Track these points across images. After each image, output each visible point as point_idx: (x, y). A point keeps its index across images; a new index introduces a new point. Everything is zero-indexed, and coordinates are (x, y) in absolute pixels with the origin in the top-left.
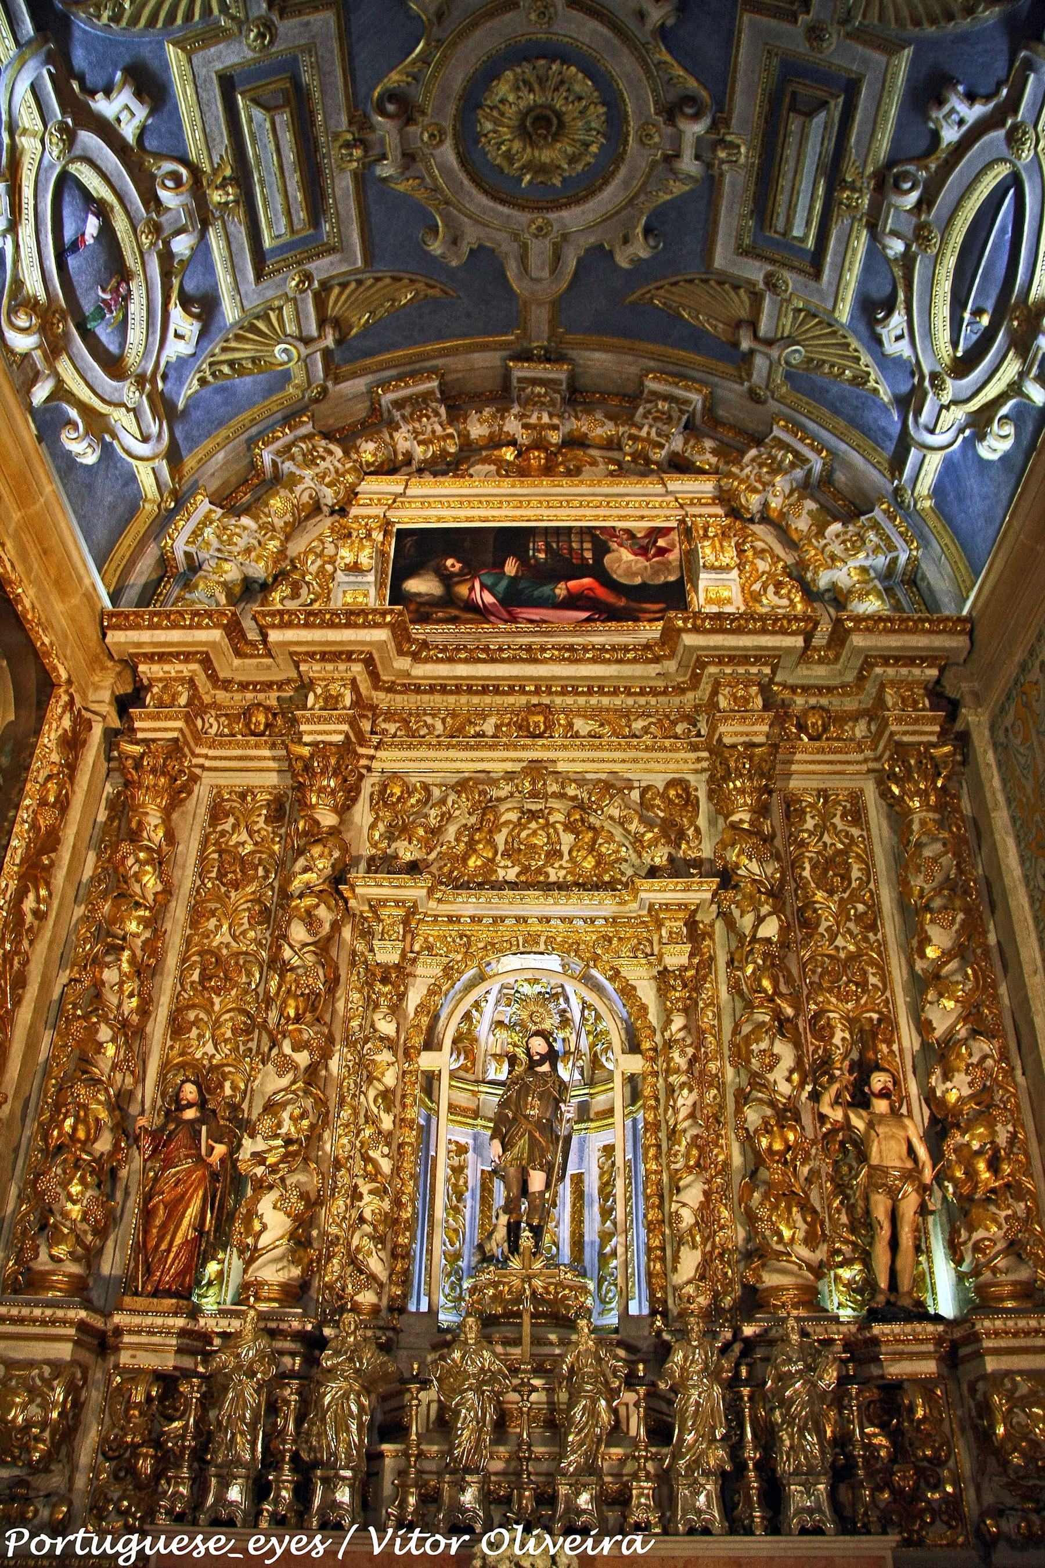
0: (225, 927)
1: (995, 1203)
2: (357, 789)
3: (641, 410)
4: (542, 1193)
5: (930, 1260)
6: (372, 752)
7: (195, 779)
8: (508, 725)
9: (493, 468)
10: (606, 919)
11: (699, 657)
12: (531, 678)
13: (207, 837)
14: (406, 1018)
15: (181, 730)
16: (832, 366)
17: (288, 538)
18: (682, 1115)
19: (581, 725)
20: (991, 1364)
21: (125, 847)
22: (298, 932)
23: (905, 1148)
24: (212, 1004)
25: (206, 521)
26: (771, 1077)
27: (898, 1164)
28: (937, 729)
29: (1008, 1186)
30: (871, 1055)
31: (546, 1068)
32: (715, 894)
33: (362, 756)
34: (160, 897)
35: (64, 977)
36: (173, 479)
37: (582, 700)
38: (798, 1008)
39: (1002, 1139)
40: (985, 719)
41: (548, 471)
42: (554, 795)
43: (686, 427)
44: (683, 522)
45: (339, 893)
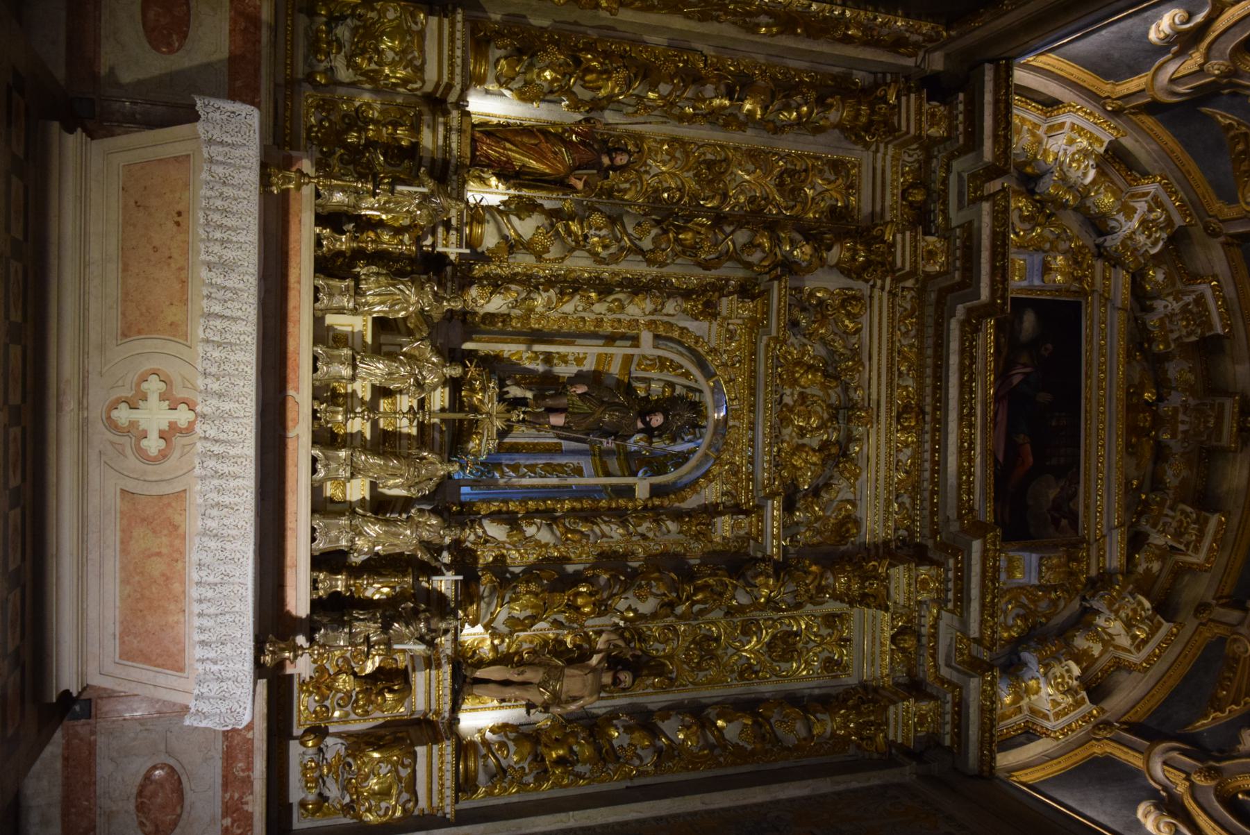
0: (747, 177)
1: (535, 759)
2: (859, 277)
3: (1189, 509)
4: (549, 423)
5: (494, 708)
6: (887, 288)
7: (867, 146)
8: (908, 396)
9: (1136, 381)
10: (751, 473)
12: (946, 415)
13: (818, 158)
14: (678, 320)
15: (908, 132)
16: (1230, 680)
17: (1076, 209)
18: (605, 528)
19: (905, 456)
20: (421, 750)
21: (812, 95)
22: (742, 237)
24: (688, 171)
25: (1092, 139)
26: (630, 594)
27: (565, 689)
28: (900, 741)
29: (546, 771)
30: (645, 672)
31: (640, 425)
32: (771, 558)
33: (884, 281)
34: (771, 125)
35: (708, 51)
36: (1133, 107)
37: (927, 456)
38: (680, 617)
39: (579, 768)
41: (1132, 429)
42: (849, 431)
43: (1171, 547)
44: (1083, 540)
45: (775, 268)
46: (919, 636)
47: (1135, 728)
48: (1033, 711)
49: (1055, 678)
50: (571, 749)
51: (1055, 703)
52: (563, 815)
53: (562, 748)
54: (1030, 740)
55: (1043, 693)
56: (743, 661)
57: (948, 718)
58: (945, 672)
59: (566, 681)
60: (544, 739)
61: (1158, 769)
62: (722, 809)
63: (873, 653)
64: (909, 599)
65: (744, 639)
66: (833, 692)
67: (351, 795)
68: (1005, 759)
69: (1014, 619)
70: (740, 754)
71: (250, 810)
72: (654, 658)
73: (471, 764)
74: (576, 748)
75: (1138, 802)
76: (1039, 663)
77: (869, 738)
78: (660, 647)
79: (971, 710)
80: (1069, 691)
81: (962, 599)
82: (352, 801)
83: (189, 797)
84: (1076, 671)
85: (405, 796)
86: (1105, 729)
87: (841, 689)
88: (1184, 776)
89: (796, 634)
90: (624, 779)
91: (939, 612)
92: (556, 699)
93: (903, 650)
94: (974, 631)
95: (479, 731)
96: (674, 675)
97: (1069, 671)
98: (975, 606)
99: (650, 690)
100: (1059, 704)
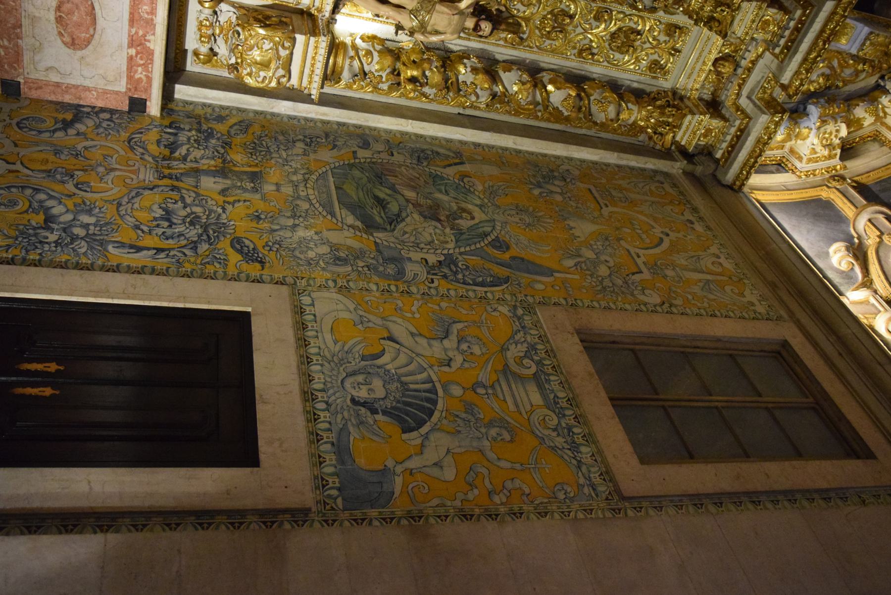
11: (813, 6)
23: (440, 29)
27: (432, 22)
28: (683, 143)
29: (399, 84)
30: (503, 27)
39: (426, 90)
40: (674, 171)
46: (737, 65)
47: (862, 189)
48: (792, 151)
49: (825, 133)
50: (424, 74)
51: (814, 151)
52: (403, 120)
53: (417, 69)
54: (778, 171)
55: (808, 141)
56: (586, 42)
57: (729, 138)
58: (743, 102)
59: (435, 15)
60: (404, 58)
61: (862, 223)
62: (527, 152)
63: (694, 68)
64: (747, 34)
65: (594, 23)
66: (648, 89)
67: (237, 58)
68: (756, 180)
69: (818, 76)
70: (556, 115)
71: (152, 47)
72: (513, 16)
73: (340, 60)
74: (427, 73)
75: (836, 241)
76: (820, 118)
77: (661, 134)
78: (522, 8)
79: (750, 138)
80: (830, 146)
81: (790, 48)
82: (237, 63)
83: (100, 22)
84: (844, 132)
85: (281, 72)
86: (838, 181)
87: (655, 89)
88: (878, 233)
89: (639, 33)
90: (458, 106)
91: (763, 52)
92: (423, 28)
93: (719, 74)
94: (785, 79)
95: (351, 35)
96: (525, 36)
97: (837, 131)
98: (798, 57)
99: (501, 42)
100: (816, 153)
